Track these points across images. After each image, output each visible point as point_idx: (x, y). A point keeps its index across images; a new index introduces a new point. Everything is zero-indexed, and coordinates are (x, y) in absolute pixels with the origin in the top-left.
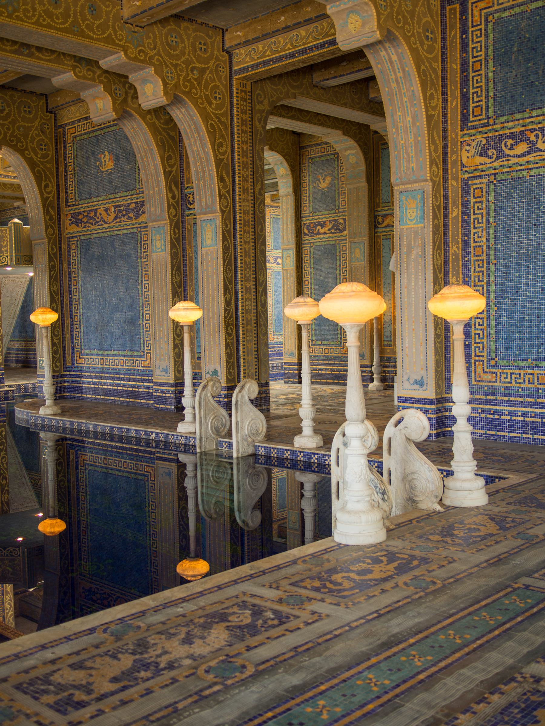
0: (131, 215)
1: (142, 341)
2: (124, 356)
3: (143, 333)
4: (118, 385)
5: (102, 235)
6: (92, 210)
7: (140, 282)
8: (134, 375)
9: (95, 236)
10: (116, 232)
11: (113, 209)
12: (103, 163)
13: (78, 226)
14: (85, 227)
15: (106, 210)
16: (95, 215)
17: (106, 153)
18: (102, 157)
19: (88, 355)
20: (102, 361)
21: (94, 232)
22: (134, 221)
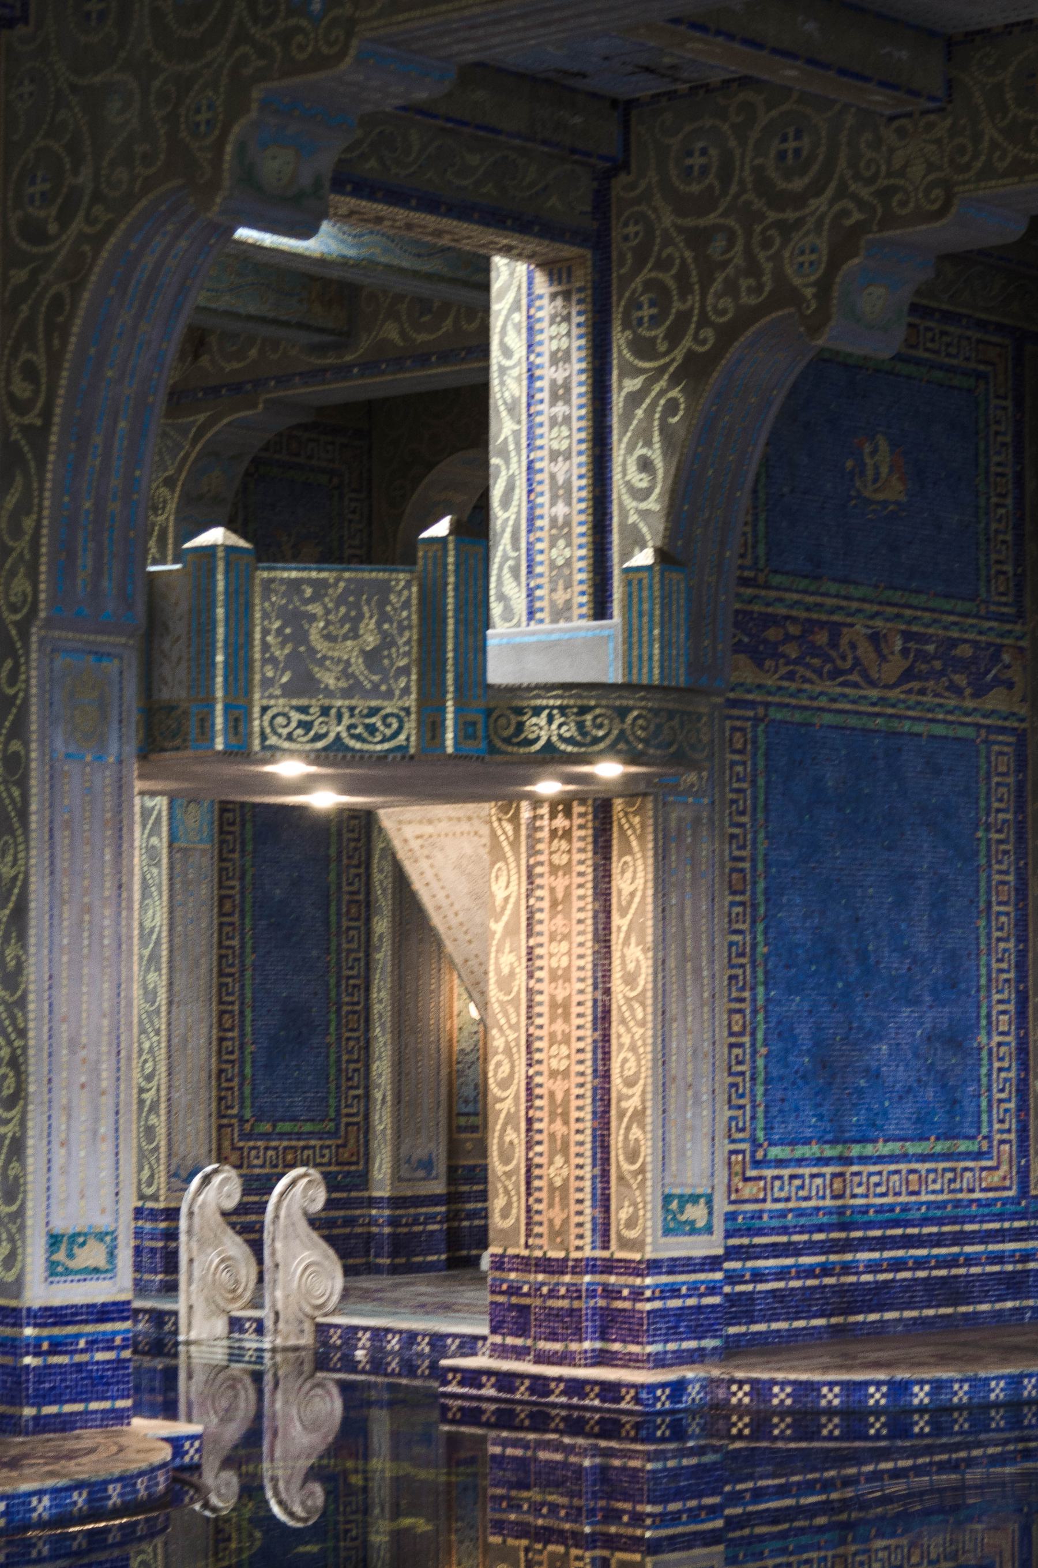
0: (960, 679)
1: (984, 1104)
2: (923, 1158)
3: (989, 1075)
4: (897, 1265)
5: (853, 721)
6: (822, 624)
7: (982, 905)
8: (955, 1220)
9: (828, 718)
10: (907, 726)
11: (898, 644)
12: (870, 473)
13: (760, 665)
14: (790, 676)
15: (875, 638)
16: (834, 644)
17: (883, 445)
18: (867, 448)
19: (780, 1163)
20: (837, 1185)
21: (823, 702)
22: (969, 704)
